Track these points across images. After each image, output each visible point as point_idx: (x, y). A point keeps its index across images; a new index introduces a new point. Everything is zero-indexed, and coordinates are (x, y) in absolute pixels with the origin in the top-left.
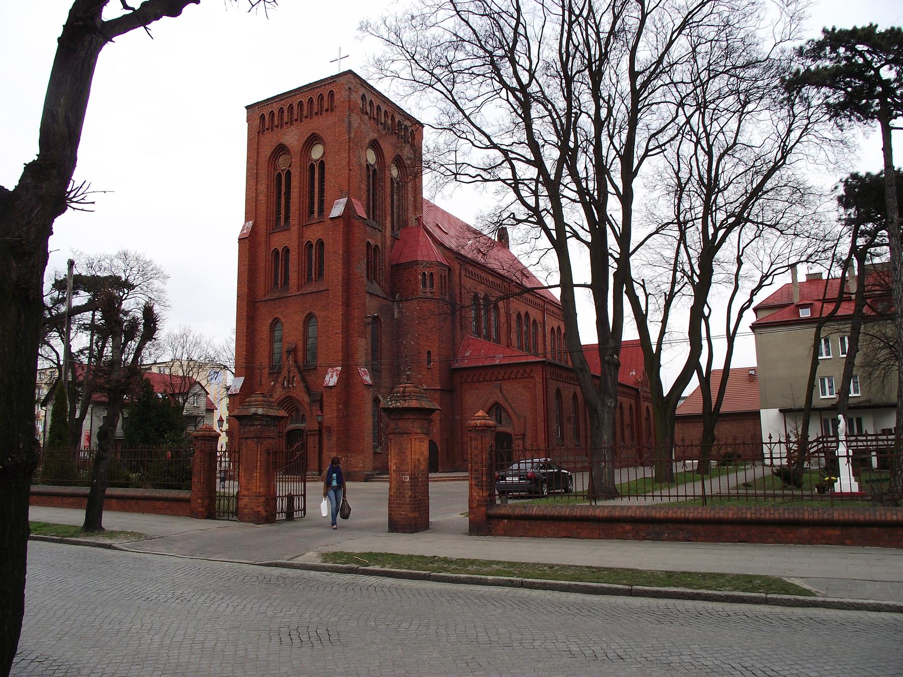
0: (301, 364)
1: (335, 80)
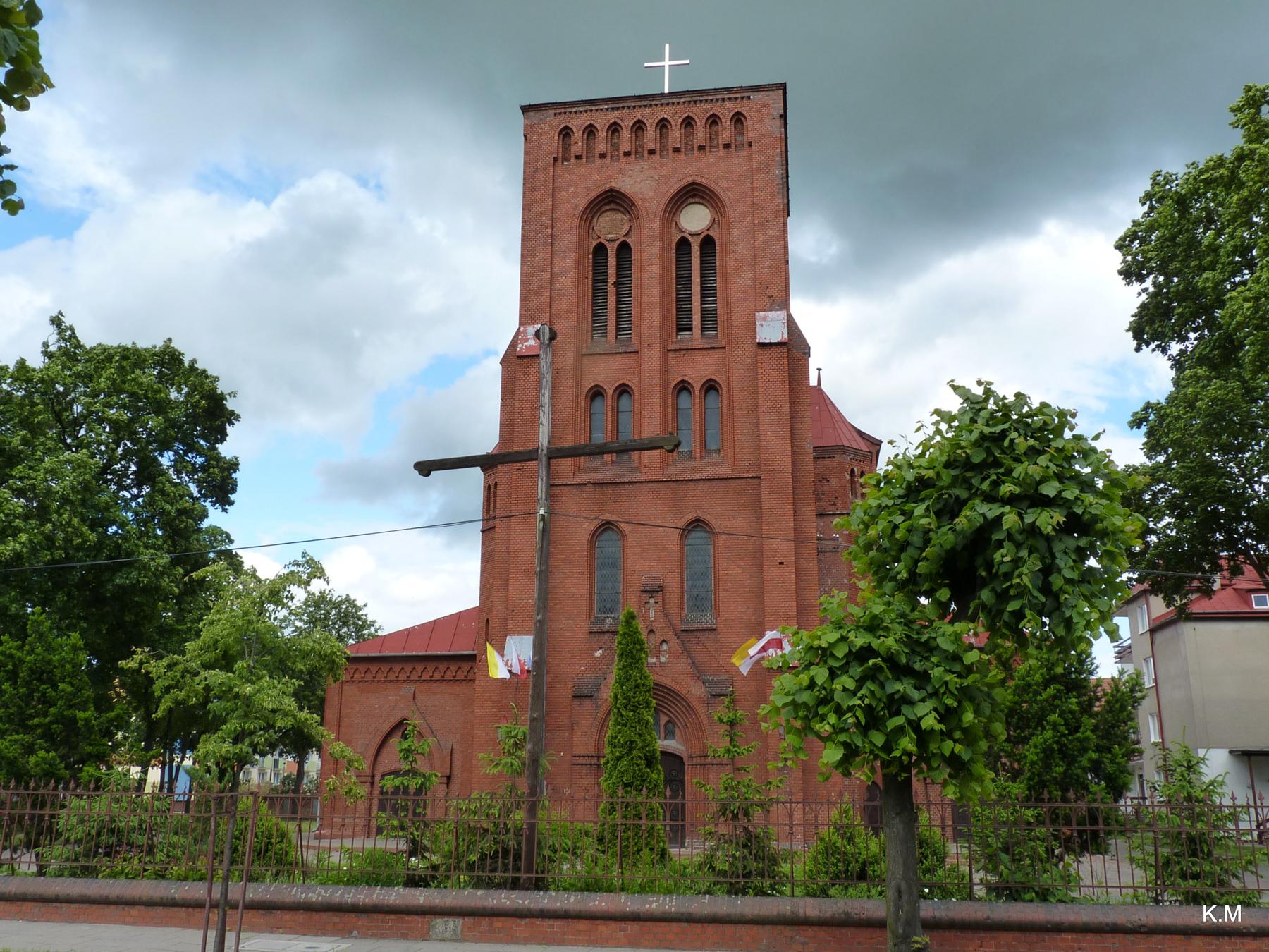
0: (676, 621)
1: (746, 94)
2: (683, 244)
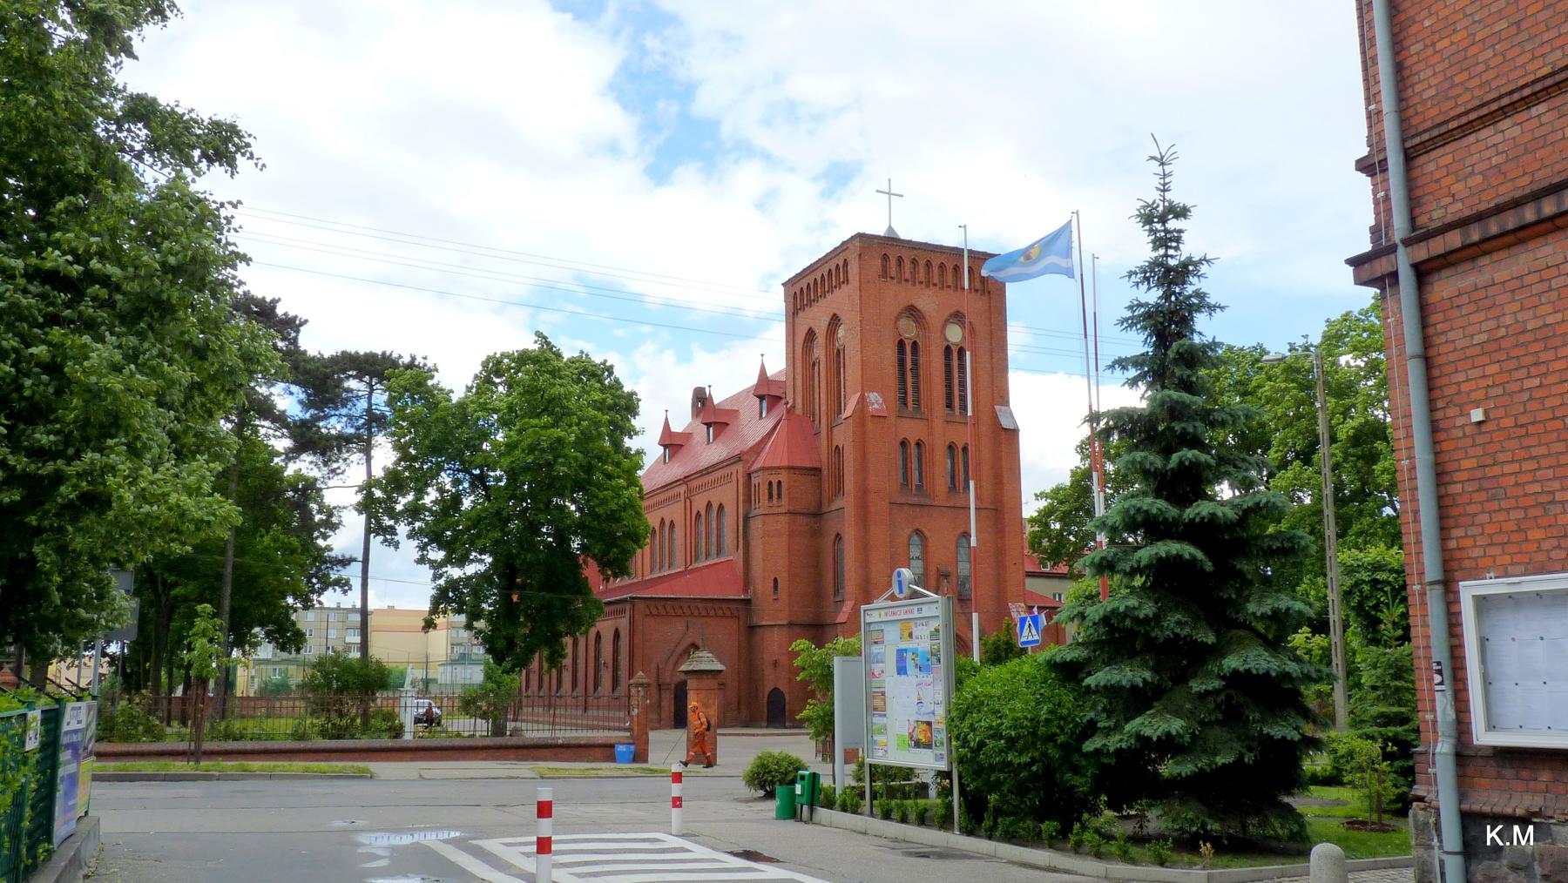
2: (948, 349)
